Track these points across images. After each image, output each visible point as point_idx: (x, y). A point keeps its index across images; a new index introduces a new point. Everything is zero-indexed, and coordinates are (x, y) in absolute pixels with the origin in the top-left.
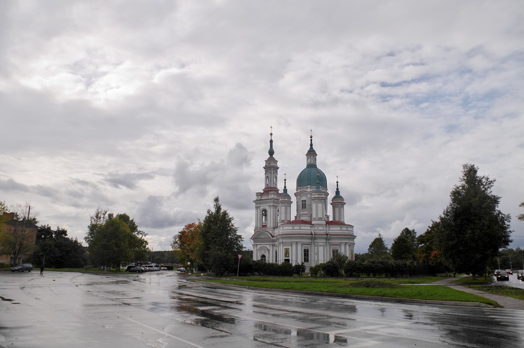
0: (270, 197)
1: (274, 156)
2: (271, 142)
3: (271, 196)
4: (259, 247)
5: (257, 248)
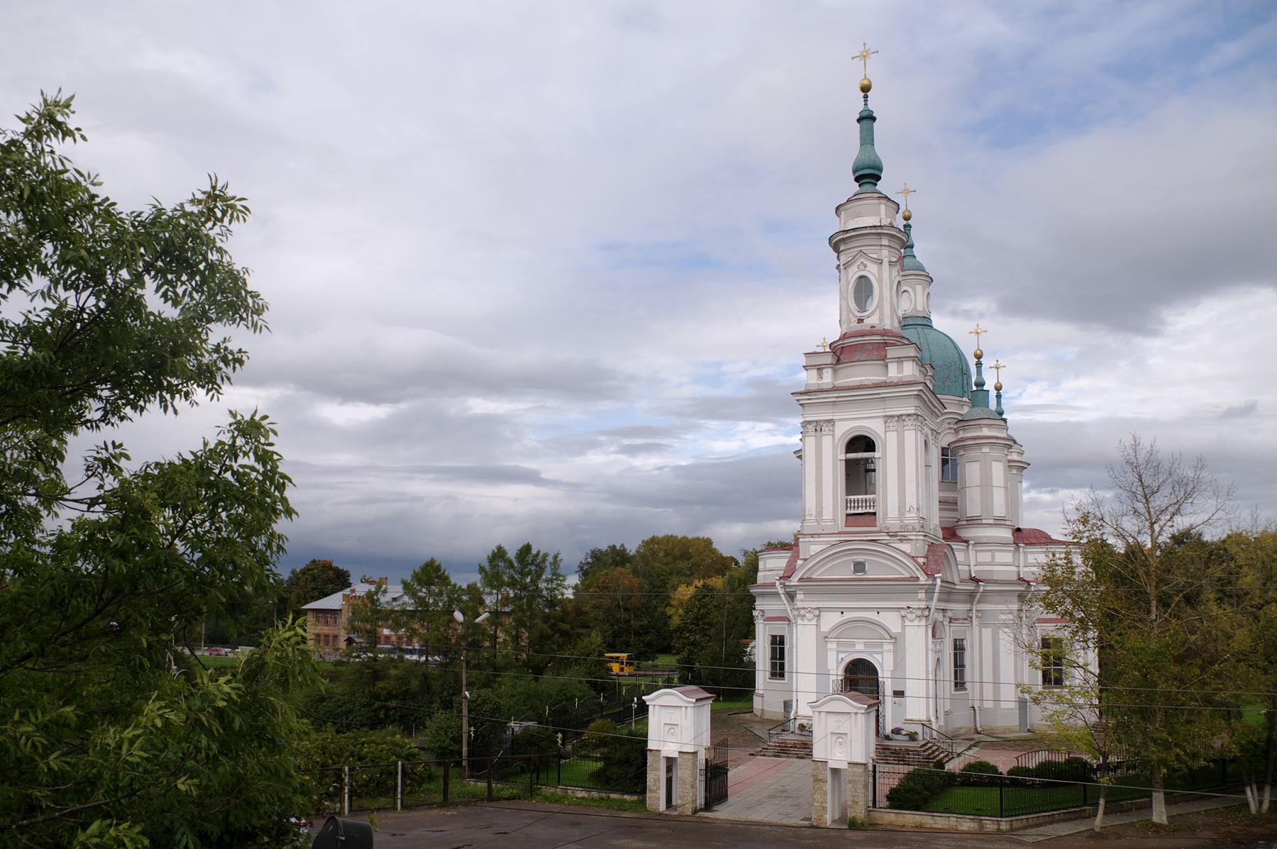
0: (893, 372)
1: (880, 186)
2: (867, 118)
3: (900, 370)
4: (830, 620)
5: (818, 626)
